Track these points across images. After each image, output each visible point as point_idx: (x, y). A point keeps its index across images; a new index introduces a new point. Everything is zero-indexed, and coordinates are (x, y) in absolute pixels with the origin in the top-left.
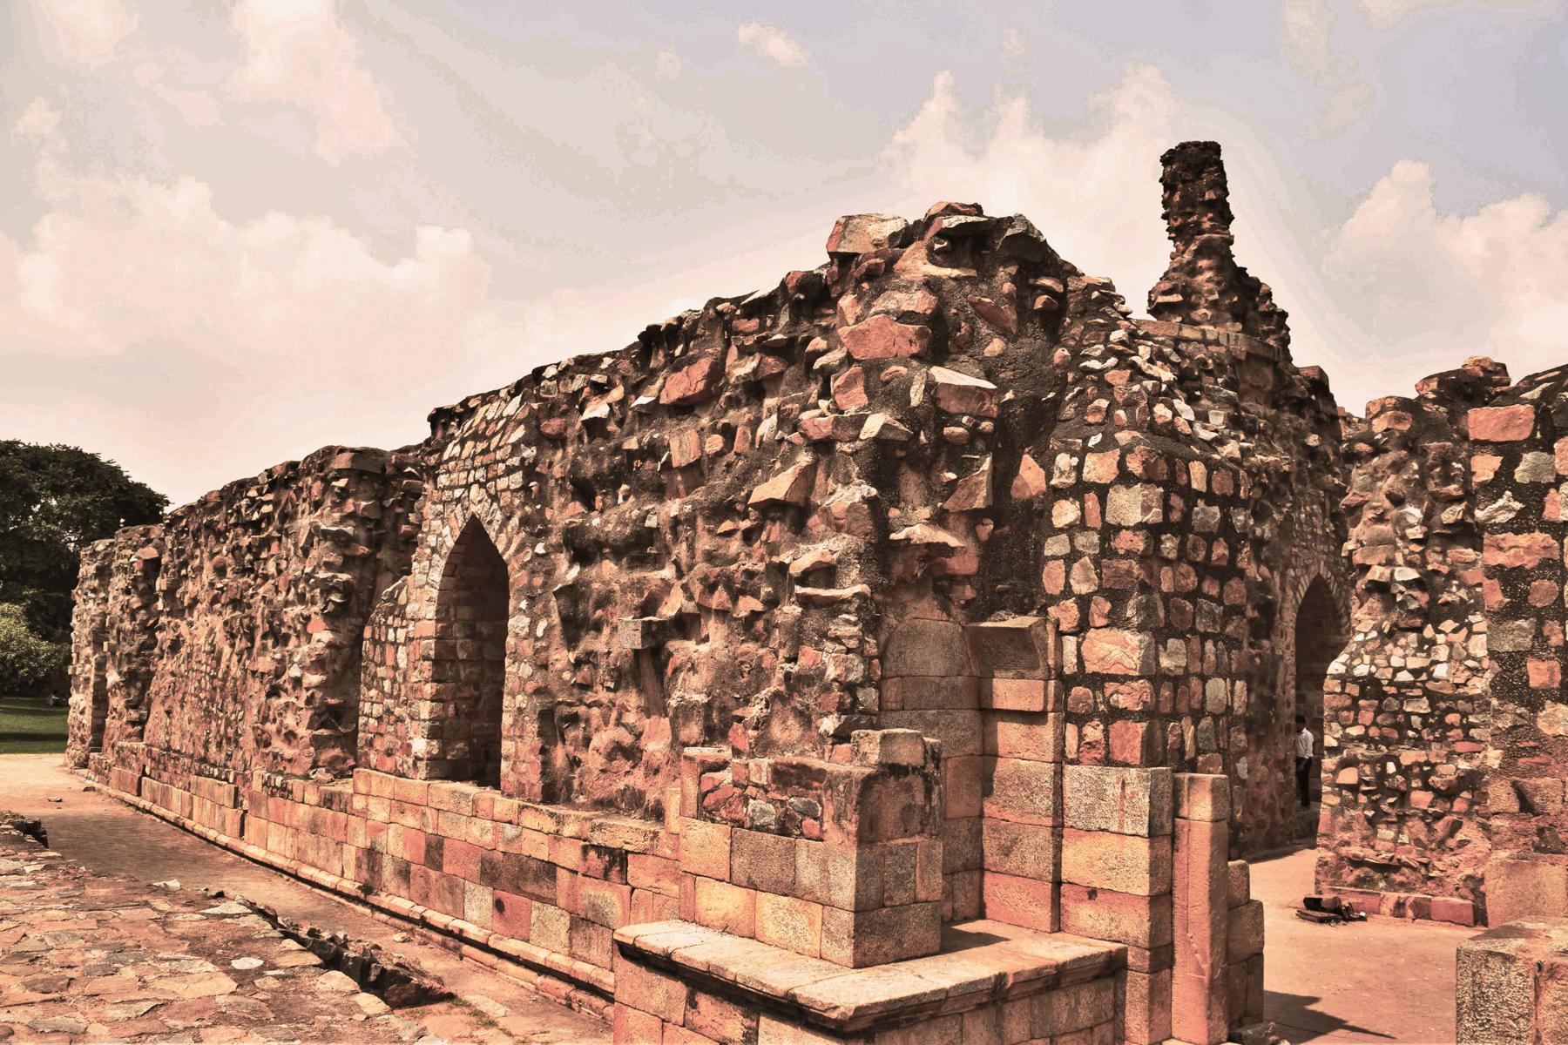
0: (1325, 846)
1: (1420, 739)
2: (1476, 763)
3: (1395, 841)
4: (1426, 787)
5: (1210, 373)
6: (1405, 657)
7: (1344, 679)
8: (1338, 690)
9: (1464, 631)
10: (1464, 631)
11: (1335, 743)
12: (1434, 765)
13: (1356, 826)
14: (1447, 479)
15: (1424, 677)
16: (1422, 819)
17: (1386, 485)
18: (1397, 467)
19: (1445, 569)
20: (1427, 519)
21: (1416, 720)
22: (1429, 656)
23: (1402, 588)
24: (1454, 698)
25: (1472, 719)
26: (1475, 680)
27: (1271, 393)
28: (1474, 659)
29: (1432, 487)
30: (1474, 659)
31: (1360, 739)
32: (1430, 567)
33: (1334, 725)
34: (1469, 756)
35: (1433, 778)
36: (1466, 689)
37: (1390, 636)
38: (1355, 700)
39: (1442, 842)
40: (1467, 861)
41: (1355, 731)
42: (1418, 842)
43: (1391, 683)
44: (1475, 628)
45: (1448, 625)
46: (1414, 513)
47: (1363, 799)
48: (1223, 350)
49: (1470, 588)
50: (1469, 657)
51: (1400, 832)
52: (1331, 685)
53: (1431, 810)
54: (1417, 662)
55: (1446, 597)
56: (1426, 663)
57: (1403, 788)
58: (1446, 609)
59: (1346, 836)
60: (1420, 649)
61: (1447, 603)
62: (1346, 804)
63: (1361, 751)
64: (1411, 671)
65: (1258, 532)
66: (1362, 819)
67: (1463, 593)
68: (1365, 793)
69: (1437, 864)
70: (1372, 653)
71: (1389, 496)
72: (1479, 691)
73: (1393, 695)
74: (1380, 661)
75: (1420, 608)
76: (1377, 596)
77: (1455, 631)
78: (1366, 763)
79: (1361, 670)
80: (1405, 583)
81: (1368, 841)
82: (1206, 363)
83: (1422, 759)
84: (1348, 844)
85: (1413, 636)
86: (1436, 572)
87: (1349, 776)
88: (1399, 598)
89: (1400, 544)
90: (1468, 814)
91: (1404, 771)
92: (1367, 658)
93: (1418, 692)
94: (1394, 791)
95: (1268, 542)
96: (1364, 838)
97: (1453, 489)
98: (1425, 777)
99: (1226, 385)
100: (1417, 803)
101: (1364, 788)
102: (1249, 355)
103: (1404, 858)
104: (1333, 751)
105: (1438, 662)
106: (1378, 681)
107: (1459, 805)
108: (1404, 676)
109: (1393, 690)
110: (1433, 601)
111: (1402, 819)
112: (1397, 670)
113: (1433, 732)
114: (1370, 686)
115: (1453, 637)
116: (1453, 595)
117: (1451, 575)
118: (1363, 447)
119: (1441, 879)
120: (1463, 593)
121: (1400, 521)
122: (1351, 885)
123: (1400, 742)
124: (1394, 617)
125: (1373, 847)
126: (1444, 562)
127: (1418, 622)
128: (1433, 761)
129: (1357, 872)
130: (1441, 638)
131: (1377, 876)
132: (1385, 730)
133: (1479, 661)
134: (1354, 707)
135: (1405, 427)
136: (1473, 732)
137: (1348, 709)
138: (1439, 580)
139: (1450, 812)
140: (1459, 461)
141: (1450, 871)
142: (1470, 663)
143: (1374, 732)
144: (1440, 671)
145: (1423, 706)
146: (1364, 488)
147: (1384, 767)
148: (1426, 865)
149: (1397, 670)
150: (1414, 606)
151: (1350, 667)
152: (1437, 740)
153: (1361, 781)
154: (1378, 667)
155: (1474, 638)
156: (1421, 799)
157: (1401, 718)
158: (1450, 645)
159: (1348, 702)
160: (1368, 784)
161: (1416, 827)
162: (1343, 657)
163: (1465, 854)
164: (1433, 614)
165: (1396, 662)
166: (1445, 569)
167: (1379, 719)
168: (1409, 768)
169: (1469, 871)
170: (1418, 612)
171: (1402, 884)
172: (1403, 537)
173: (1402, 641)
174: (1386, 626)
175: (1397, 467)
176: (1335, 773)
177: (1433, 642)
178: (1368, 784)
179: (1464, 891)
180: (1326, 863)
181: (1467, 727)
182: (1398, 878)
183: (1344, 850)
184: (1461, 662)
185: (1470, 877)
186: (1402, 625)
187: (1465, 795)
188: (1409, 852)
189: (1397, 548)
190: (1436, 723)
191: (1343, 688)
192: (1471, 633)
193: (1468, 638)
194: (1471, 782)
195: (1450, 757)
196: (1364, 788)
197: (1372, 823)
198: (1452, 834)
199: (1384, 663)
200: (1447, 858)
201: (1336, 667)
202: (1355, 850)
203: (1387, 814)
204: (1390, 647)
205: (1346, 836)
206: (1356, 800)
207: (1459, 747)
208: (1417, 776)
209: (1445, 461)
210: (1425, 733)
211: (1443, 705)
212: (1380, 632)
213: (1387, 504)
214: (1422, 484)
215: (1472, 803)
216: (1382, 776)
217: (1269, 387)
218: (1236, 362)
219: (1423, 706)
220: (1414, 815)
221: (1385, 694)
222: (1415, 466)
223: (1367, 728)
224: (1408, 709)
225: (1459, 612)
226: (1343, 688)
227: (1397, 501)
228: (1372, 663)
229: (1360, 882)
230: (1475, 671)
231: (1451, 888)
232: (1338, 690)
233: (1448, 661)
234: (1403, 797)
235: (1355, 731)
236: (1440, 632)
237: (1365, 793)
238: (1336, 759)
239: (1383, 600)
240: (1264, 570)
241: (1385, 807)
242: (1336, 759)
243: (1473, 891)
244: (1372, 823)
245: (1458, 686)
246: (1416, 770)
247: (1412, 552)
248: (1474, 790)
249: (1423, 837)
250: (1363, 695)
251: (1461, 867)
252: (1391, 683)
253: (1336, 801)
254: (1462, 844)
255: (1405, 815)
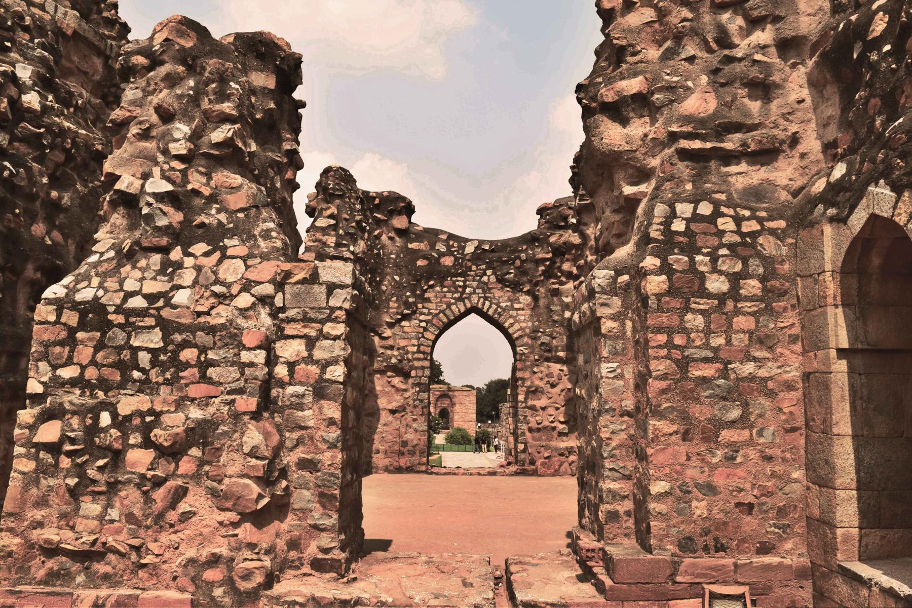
0: (11, 530)
1: (147, 381)
2: (211, 410)
3: (101, 518)
4: (147, 443)
5: (26, 29)
6: (142, 280)
7: (60, 305)
8: (52, 318)
9: (217, 255)
10: (217, 255)
11: (40, 389)
12: (158, 415)
13: (54, 500)
14: (222, 96)
15: (161, 303)
16: (138, 486)
17: (155, 99)
18: (172, 81)
19: (206, 191)
20: (195, 137)
21: (144, 358)
22: (171, 279)
23: (151, 200)
24: (192, 329)
25: (211, 355)
26: (221, 309)
27: (99, 85)
28: (223, 284)
29: (205, 104)
30: (223, 284)
31: (74, 382)
32: (190, 187)
33: (43, 366)
34: (204, 402)
35: (157, 431)
36: (208, 319)
37: (128, 256)
38: (72, 331)
39: (161, 515)
40: (191, 539)
41: (67, 373)
42: (130, 517)
43: (119, 310)
44: (229, 252)
45: (200, 248)
46: (181, 129)
47: (65, 462)
48: (47, 17)
49: (231, 213)
50: (217, 282)
51: (109, 505)
52: (45, 312)
53: (150, 474)
54: (151, 287)
55: (203, 218)
56: (166, 287)
57: (117, 446)
58: (200, 231)
59: (39, 514)
60: (162, 271)
61: (202, 225)
62: (43, 470)
63: (73, 398)
64: (146, 297)
65: (54, 194)
66: (62, 491)
67: (223, 217)
68: (69, 454)
69: (152, 546)
70: (104, 276)
71: (159, 109)
72: (222, 321)
73: (120, 326)
74: (112, 284)
75: (170, 226)
76: (121, 210)
77: (207, 254)
78: (74, 413)
79: (85, 294)
80: (155, 195)
81: (67, 520)
82: (22, 18)
83: (145, 407)
84: (40, 525)
85: (156, 258)
86: (196, 193)
87: (50, 432)
88: (145, 211)
89: (161, 158)
90: (196, 477)
91: (121, 423)
92: (96, 281)
93: (150, 321)
94: (106, 450)
95: (66, 210)
96: (63, 516)
97: (227, 107)
98: (146, 429)
99: (43, 46)
100: (133, 465)
101: (68, 447)
102: (75, 32)
103: (111, 541)
104: (37, 399)
105: (180, 287)
106: (104, 306)
107: (186, 466)
108: (137, 302)
109: (120, 319)
110: (187, 222)
111: (113, 487)
112: (129, 295)
113: (163, 372)
114: (93, 315)
115: (204, 261)
116: (213, 217)
117: (213, 199)
118: (140, 60)
119: (155, 566)
120: (223, 217)
121: (167, 137)
122: (39, 583)
123: (122, 386)
124: (137, 234)
125: (72, 528)
126: (208, 184)
127: (164, 241)
128: (158, 408)
129: (51, 564)
130: (189, 262)
131: (75, 567)
132: (106, 371)
133: (228, 286)
134: (71, 341)
135: (189, 44)
136: (211, 372)
137: (61, 343)
138: (198, 202)
139: (174, 475)
140: (238, 83)
141: (167, 555)
142: (218, 289)
143: (91, 373)
144: (181, 297)
145: (154, 339)
146: (133, 103)
147: (96, 419)
148: (137, 549)
149: (129, 295)
150: (162, 222)
151: (72, 290)
152: (167, 382)
153: (64, 438)
154: (106, 291)
155: (227, 262)
156: (139, 459)
157: (126, 355)
158: (198, 269)
159: (63, 334)
160: (73, 441)
161: (131, 496)
162: (68, 280)
163: (188, 531)
164: (182, 236)
165: (130, 285)
166: (206, 191)
167: (100, 356)
168: (128, 418)
169: (191, 553)
170: (168, 230)
171: (106, 577)
172: (165, 152)
173: (143, 263)
174: (127, 245)
175: (172, 81)
176: (33, 428)
177: (179, 265)
178: (73, 441)
179: (184, 581)
180: (10, 554)
181: (204, 365)
182: (101, 568)
183: (37, 535)
184: (207, 287)
185: (192, 561)
186: (145, 243)
187: (195, 452)
188: (118, 532)
189: (157, 163)
190: (168, 360)
191: (59, 316)
192: (224, 257)
193: (220, 262)
194: (200, 434)
195: (179, 405)
196: (68, 447)
197: (74, 494)
198: (173, 506)
199: (116, 286)
200: (166, 538)
201: (55, 291)
202: (50, 534)
203: (94, 482)
204: (128, 268)
205: (39, 514)
206: (56, 465)
207: (195, 391)
208: (136, 429)
209: (223, 79)
210: (154, 375)
211: (178, 337)
212: (119, 252)
213: (154, 118)
214: (195, 100)
215: (202, 463)
216: (93, 430)
217: (97, 78)
218: (59, 32)
219: (154, 339)
220: (129, 481)
221: (110, 325)
222: (192, 83)
223: (83, 368)
224: (135, 343)
225: (215, 237)
226: (59, 316)
227: (166, 116)
228: (101, 286)
229: (52, 577)
230: (222, 298)
231: (168, 577)
232: (52, 318)
233: (192, 286)
234: (117, 457)
235: (67, 373)
236: (187, 254)
237: (69, 454)
238: (37, 410)
239: (129, 216)
240: (56, 235)
241: (92, 473)
242: (37, 410)
243: (193, 580)
244: (74, 494)
245: (199, 314)
246: (137, 421)
247: (173, 169)
248: (205, 445)
249: (137, 512)
250: (83, 325)
251: (182, 548)
252: (119, 310)
253: (28, 466)
254: (186, 517)
255: (118, 482)
